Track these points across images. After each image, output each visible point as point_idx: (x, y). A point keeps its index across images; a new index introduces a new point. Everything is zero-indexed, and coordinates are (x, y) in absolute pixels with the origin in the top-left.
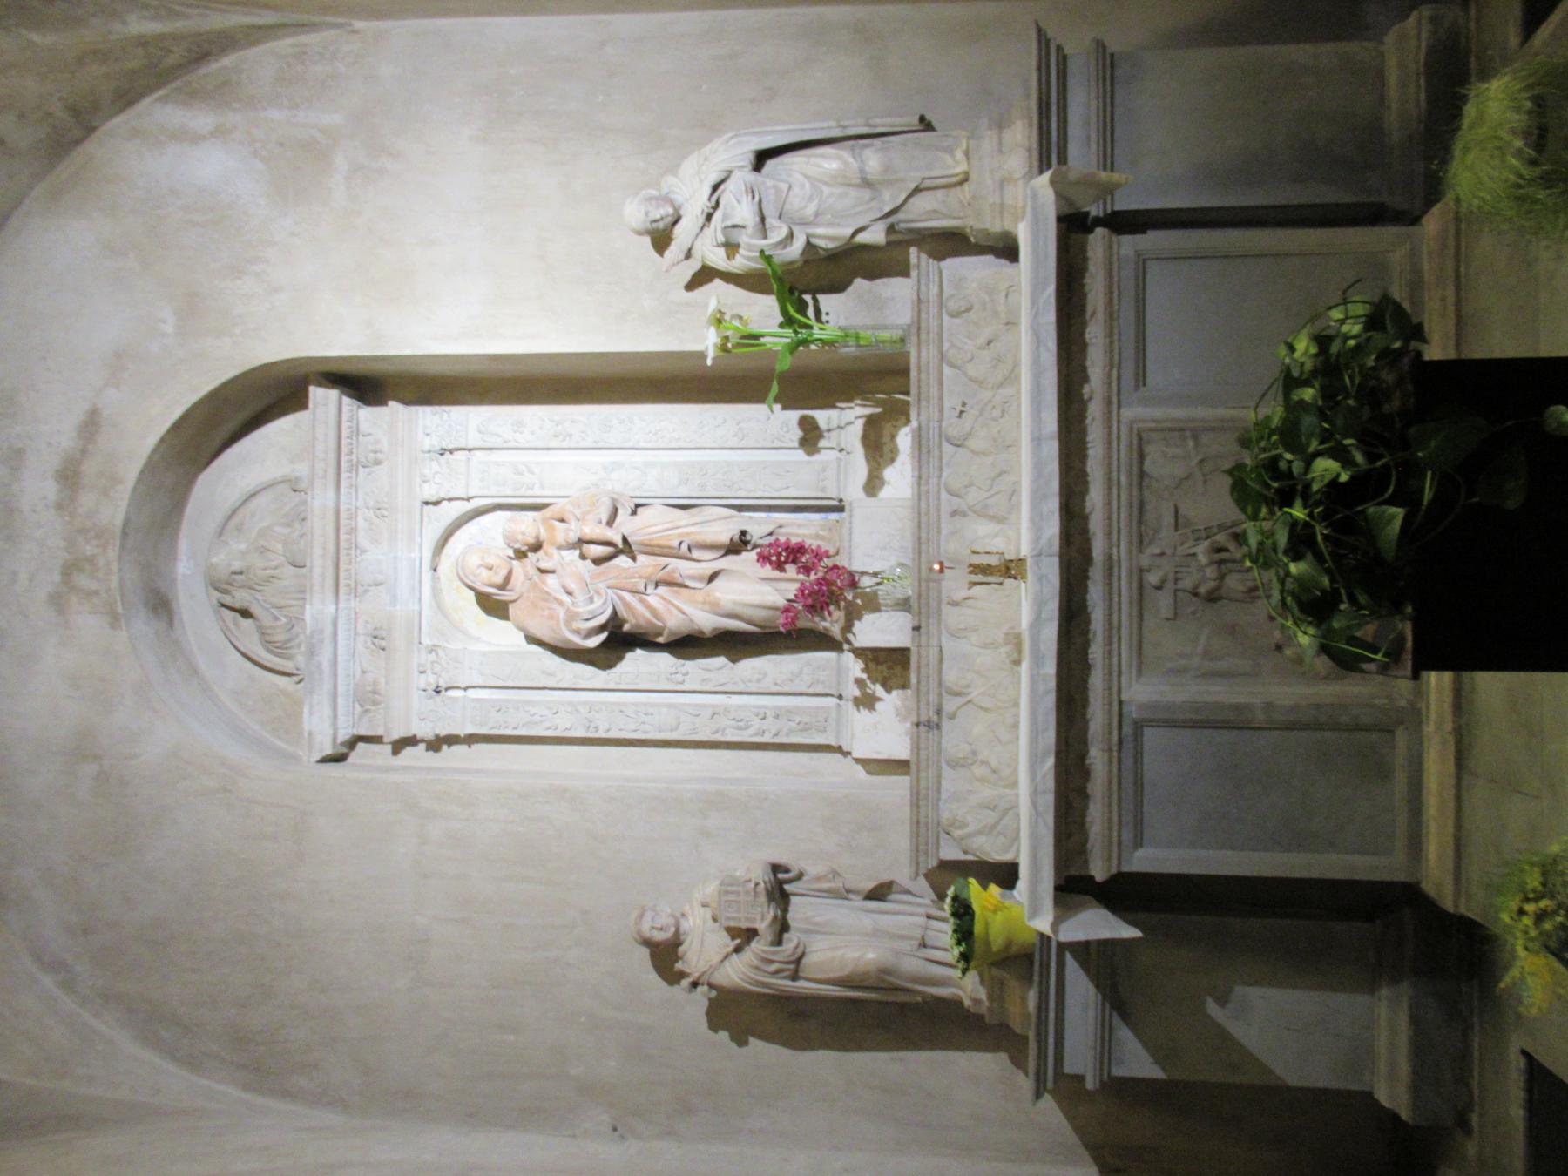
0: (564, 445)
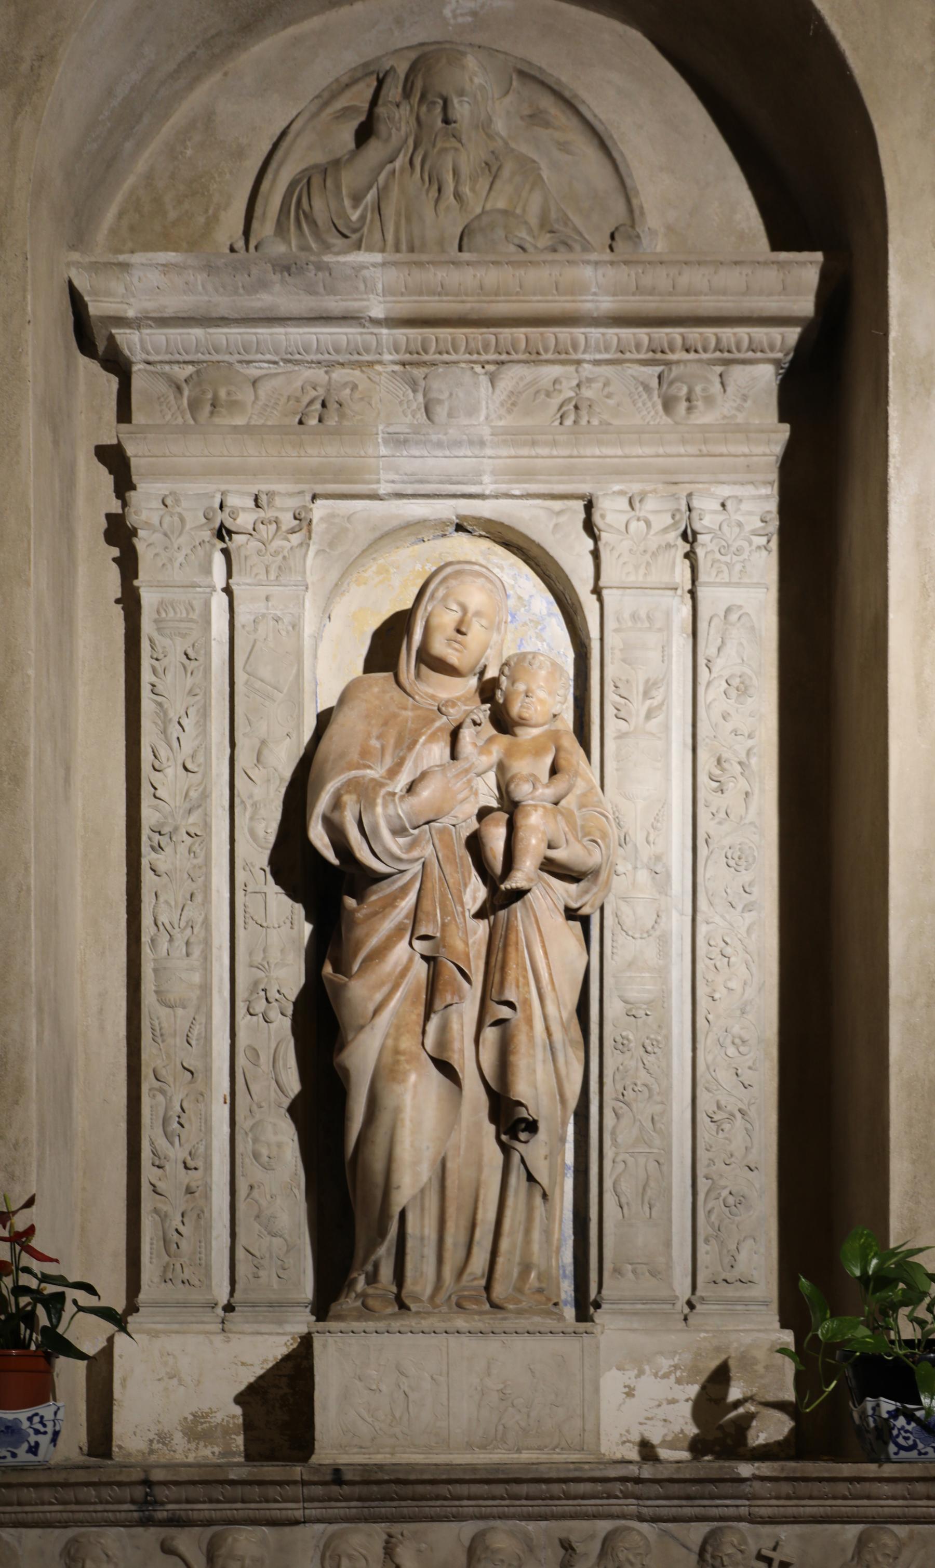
0: (702, 778)
